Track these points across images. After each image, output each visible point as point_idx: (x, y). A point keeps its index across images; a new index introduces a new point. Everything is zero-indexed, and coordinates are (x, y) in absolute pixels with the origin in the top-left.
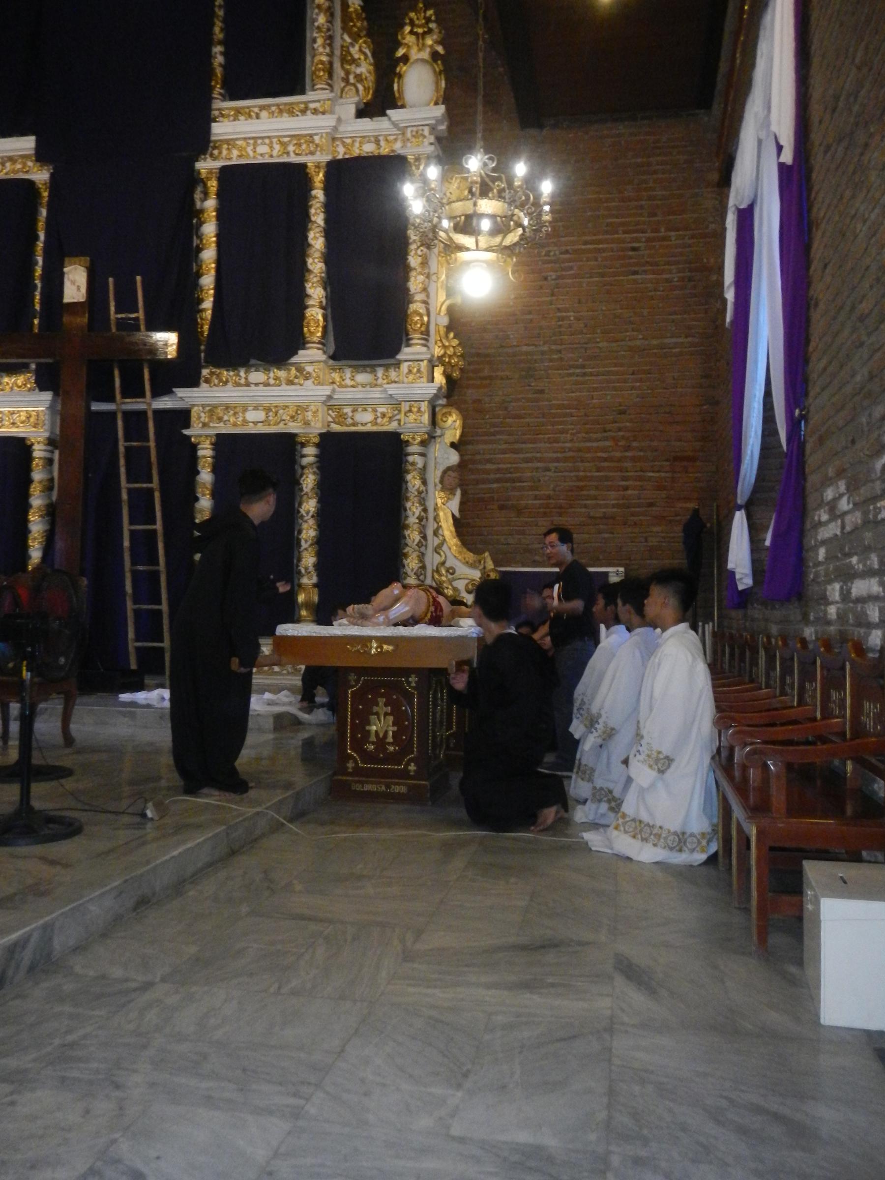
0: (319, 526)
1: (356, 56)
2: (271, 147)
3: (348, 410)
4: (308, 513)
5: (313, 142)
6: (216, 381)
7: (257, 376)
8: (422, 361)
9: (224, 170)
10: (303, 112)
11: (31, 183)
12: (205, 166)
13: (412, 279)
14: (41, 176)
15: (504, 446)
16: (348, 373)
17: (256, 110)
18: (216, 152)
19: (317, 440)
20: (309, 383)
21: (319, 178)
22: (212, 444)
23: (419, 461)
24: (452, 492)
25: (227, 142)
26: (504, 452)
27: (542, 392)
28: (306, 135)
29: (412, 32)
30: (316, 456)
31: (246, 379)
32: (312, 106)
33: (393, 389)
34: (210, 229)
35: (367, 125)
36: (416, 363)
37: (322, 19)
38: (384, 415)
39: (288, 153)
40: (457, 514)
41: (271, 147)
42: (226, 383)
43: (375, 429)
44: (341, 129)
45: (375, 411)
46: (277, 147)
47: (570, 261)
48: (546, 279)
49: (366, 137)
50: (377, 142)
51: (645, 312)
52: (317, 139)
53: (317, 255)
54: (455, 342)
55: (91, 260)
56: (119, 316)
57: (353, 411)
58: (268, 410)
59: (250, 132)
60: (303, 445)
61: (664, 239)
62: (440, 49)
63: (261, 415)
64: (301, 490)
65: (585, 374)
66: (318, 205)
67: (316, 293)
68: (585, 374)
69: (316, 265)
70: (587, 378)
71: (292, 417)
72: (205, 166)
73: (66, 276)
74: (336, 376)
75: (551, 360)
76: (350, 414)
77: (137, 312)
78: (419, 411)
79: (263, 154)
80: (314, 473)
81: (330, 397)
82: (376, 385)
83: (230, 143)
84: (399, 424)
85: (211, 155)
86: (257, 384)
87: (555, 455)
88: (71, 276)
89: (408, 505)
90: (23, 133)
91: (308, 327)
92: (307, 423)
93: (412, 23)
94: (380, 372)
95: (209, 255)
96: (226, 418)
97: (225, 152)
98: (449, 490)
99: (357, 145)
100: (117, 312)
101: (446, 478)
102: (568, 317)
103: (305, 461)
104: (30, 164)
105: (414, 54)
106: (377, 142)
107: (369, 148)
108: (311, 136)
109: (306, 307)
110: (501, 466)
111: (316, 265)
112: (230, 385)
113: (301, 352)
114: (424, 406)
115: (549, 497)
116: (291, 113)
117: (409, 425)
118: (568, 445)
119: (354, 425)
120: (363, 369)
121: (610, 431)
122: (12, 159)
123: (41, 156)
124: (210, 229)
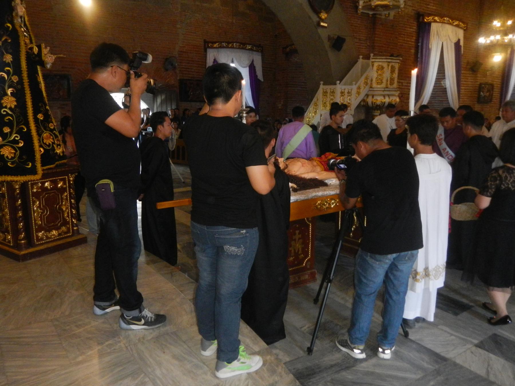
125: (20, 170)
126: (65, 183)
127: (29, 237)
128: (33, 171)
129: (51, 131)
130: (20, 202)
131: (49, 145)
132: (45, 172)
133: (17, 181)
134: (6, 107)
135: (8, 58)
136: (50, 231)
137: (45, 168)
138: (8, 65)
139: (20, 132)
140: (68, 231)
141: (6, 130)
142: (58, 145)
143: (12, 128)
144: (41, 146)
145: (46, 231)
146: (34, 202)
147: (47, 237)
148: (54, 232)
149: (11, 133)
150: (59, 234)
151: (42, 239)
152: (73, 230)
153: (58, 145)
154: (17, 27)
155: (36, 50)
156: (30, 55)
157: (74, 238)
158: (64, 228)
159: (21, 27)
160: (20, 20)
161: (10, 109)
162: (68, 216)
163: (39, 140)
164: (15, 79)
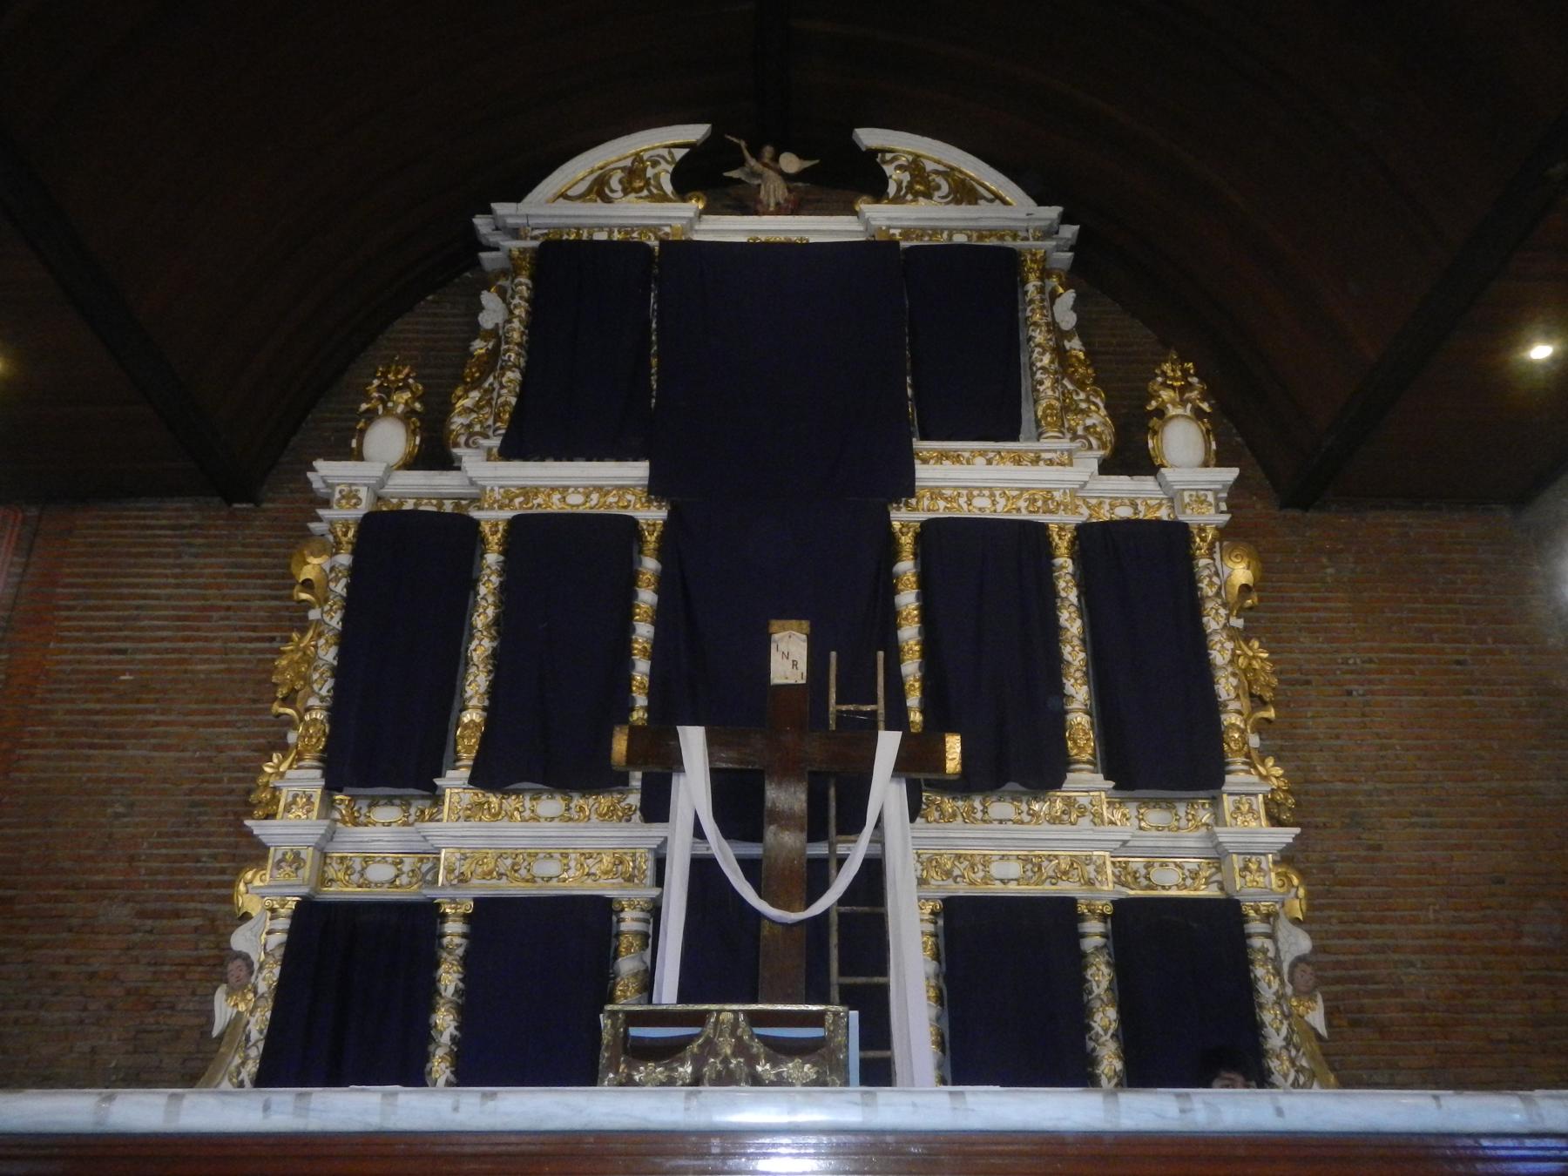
0: (1124, 1052)
1: (1083, 406)
2: (994, 503)
3: (1137, 863)
4: (1106, 1031)
5: (1052, 498)
6: (937, 814)
7: (1001, 808)
8: (1255, 795)
9: (927, 525)
10: (1036, 461)
11: (633, 522)
12: (904, 518)
13: (1223, 681)
14: (652, 516)
15: (1338, 928)
16: (1131, 809)
17: (967, 455)
18: (913, 501)
19: (1108, 910)
20: (1085, 822)
21: (1062, 544)
22: (933, 913)
23: (1268, 944)
24: (1309, 994)
25: (930, 488)
26: (1339, 935)
27: (1379, 848)
28: (1042, 490)
29: (1165, 385)
30: (1104, 935)
31: (985, 812)
32: (1045, 456)
33: (1224, 835)
34: (908, 600)
35: (1122, 484)
36: (1244, 798)
37: (1046, 359)
38: (1195, 875)
39: (1019, 510)
40: (1322, 1030)
41: (994, 503)
42: (954, 815)
43: (1184, 893)
44: (1089, 486)
46: (1002, 502)
47: (1381, 672)
48: (1349, 693)
49: (1126, 498)
50: (1134, 505)
51: (1495, 745)
52: (1058, 495)
53: (1076, 642)
54: (1279, 771)
55: (812, 626)
56: (844, 708)
57: (1148, 866)
58: (1026, 860)
59: (962, 479)
60: (1081, 918)
61: (1493, 652)
63: (1014, 869)
64: (1091, 992)
65: (1433, 826)
66: (1069, 577)
67: (1078, 691)
68: (1433, 826)
69: (1074, 655)
70: (1437, 830)
71: (1065, 873)
72: (904, 518)
73: (773, 646)
74: (1118, 816)
75: (1382, 804)
76: (1143, 871)
77: (875, 702)
78: (1260, 869)
79: (981, 507)
80: (1108, 964)
81: (1125, 842)
82: (1179, 828)
83: (936, 493)
84: (1222, 889)
85: (907, 505)
86: (1001, 822)
87: (1418, 942)
88: (782, 647)
89: (1268, 1016)
90: (620, 456)
91: (1075, 742)
92: (1090, 883)
93: (1164, 374)
94: (1182, 809)
95: (909, 633)
96: (956, 872)
97: (926, 502)
98: (1305, 994)
99: (1107, 507)
100: (838, 703)
101: (1298, 974)
102: (1393, 747)
103: (1089, 944)
104: (629, 497)
106: (1134, 505)
107: (1124, 512)
108: (1049, 491)
109: (1067, 712)
110: (1341, 958)
111: (1074, 655)
112: (960, 819)
113: (1070, 776)
115: (1423, 1009)
117: (1245, 890)
118: (1431, 927)
119: (1149, 887)
120: (1156, 803)
121: (1489, 908)
122: (598, 489)
123: (656, 489)
124: (908, 600)
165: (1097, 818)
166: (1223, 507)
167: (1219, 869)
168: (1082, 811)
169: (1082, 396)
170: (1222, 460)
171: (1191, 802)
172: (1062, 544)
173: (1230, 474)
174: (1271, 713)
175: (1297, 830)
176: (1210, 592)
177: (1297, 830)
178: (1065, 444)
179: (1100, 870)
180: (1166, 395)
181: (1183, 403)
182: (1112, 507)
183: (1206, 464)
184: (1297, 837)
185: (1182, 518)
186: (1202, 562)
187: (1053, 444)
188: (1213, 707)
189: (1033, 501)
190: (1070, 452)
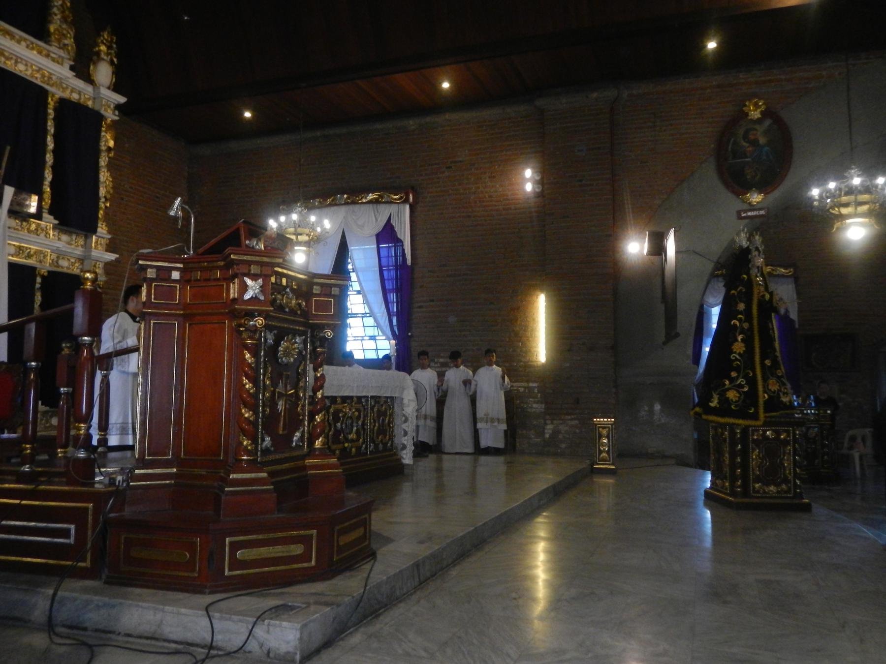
10: (48, 56)
19: (46, 274)
32: (52, 55)
33: (95, 253)
35: (80, 84)
38: (73, 264)
45: (69, 260)
48: (122, 199)
50: (80, 93)
58: (20, 248)
62: (115, 60)
69: (49, 158)
94: (74, 237)
105: (103, 56)
107: (75, 97)
108: (51, 74)
111: (49, 158)
114: (101, 265)
116: (40, 53)
125: (742, 413)
126: (788, 436)
127: (745, 486)
128: (755, 417)
129: (779, 377)
130: (739, 447)
131: (774, 392)
132: (768, 419)
133: (738, 425)
134: (735, 353)
135: (741, 306)
136: (768, 485)
137: (767, 415)
138: (741, 313)
139: (746, 377)
140: (788, 491)
141: (734, 374)
142: (784, 393)
143: (738, 371)
144: (765, 392)
145: (764, 484)
146: (754, 450)
147: (765, 492)
148: (772, 488)
149: (738, 378)
150: (778, 492)
151: (758, 492)
152: (795, 492)
153: (784, 393)
154: (753, 277)
155: (767, 296)
156: (761, 303)
157: (796, 501)
158: (784, 486)
159: (757, 276)
160: (756, 270)
161: (740, 354)
162: (790, 473)
163: (764, 387)
164: (746, 325)
165: (47, 235)
166: (117, 113)
167: (82, 264)
168: (43, 230)
169: (64, 26)
170: (116, 88)
171: (78, 235)
172: (51, 103)
173: (122, 100)
174: (108, 205)
175: (117, 256)
176: (103, 148)
177: (117, 256)
178: (61, 53)
179: (45, 256)
180: (103, 48)
181: (108, 54)
182: (72, 92)
183: (109, 88)
184: (117, 260)
185: (103, 112)
186: (103, 134)
187: (54, 49)
188: (97, 198)
189: (43, 76)
190: (63, 58)
